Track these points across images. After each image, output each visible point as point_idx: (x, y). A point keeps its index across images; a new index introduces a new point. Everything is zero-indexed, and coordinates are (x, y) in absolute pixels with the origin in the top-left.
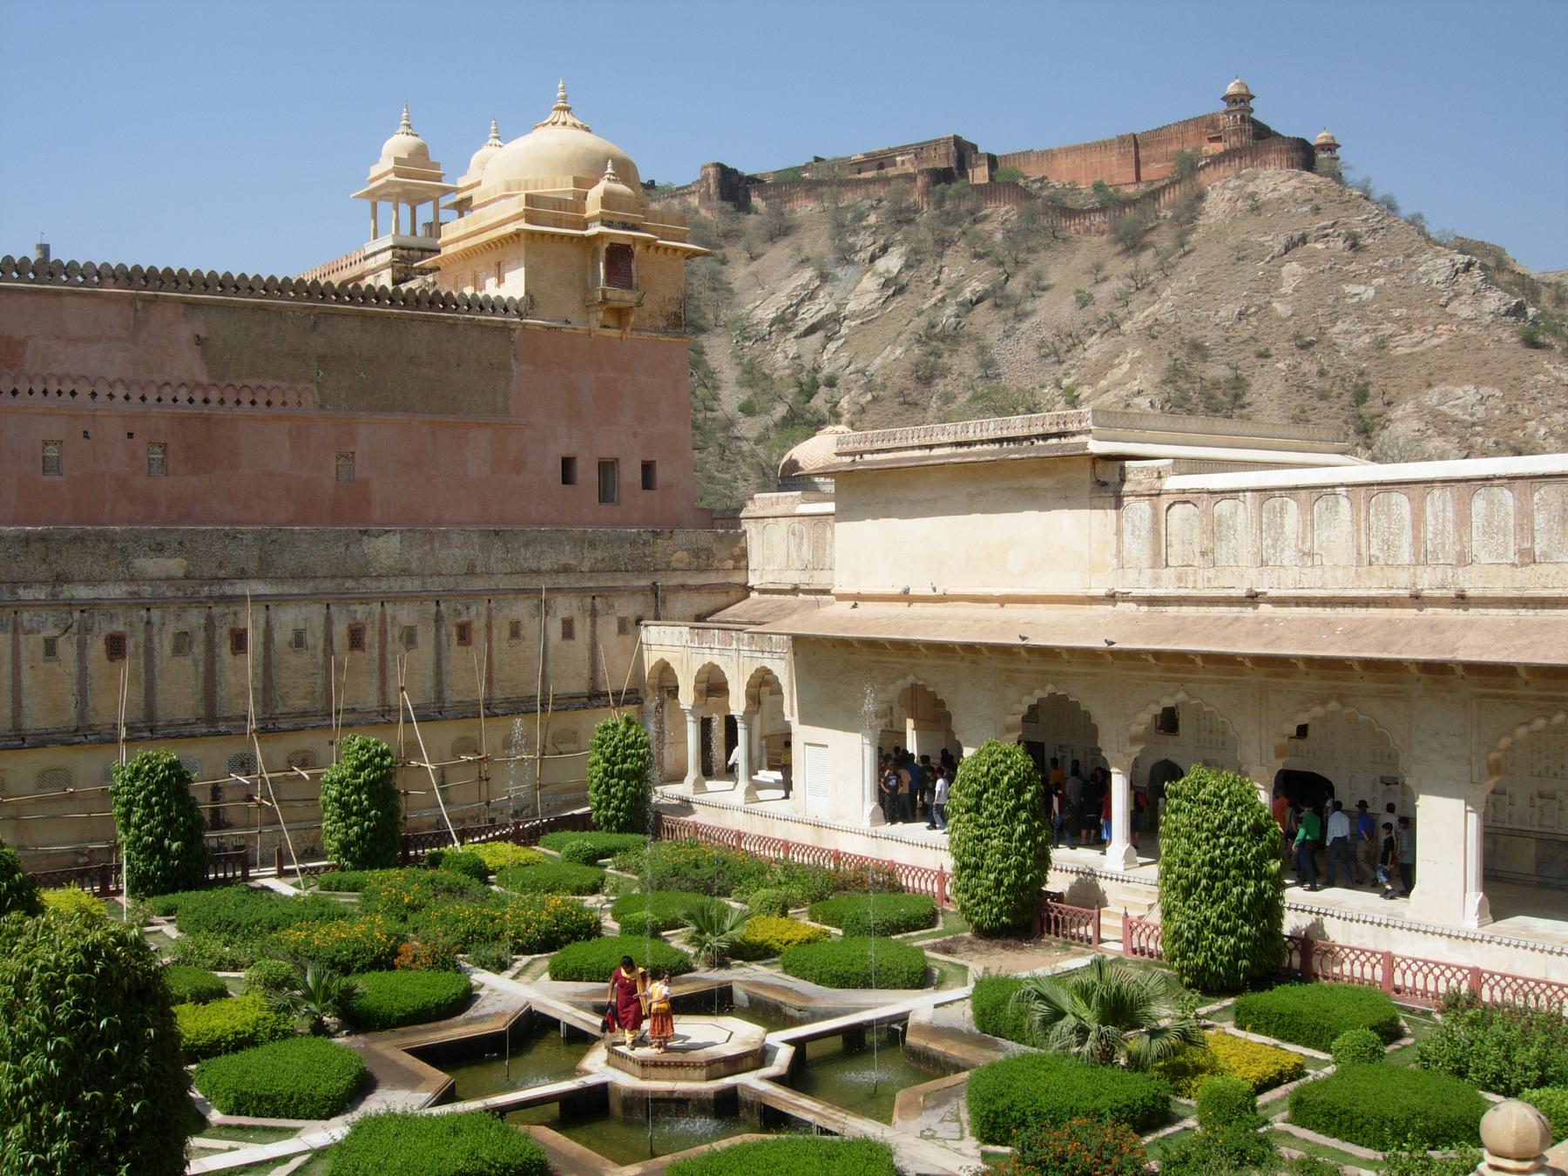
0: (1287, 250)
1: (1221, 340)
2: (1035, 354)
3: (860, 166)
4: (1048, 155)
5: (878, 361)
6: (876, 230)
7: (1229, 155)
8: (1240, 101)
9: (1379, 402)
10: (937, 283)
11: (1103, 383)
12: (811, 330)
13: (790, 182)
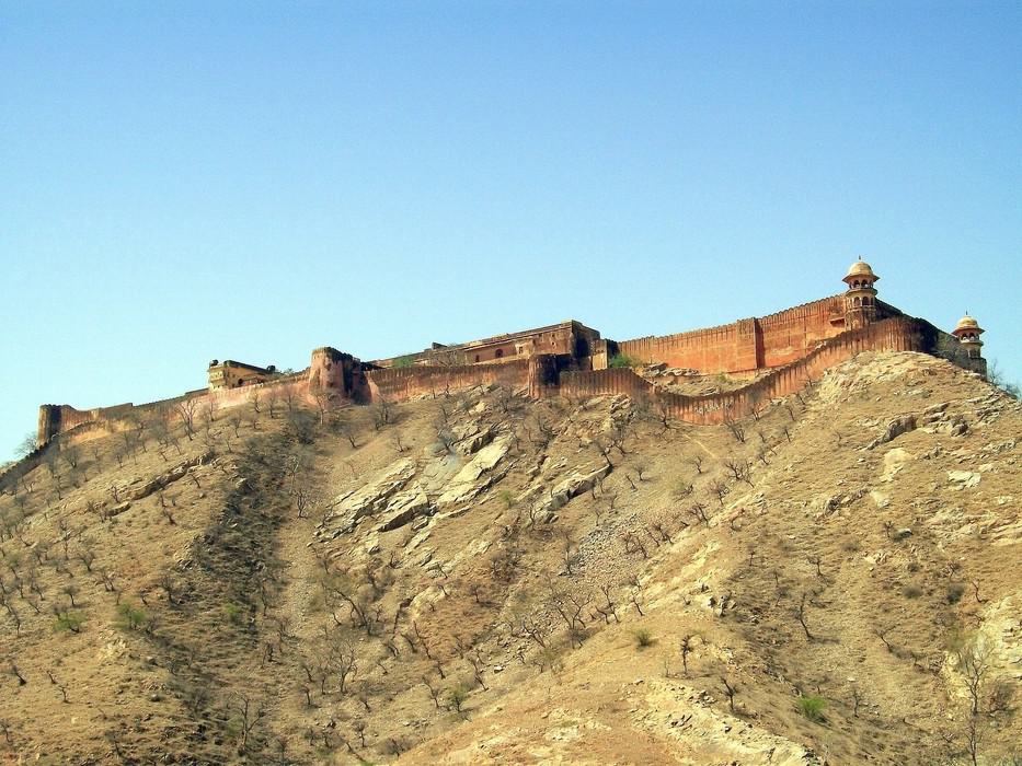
0: (894, 434)
1: (809, 532)
2: (622, 549)
3: (476, 352)
4: (670, 341)
5: (459, 556)
6: (482, 419)
7: (845, 338)
8: (863, 282)
9: (973, 599)
10: (535, 474)
11: (676, 580)
12: (397, 523)
13: (410, 370)
